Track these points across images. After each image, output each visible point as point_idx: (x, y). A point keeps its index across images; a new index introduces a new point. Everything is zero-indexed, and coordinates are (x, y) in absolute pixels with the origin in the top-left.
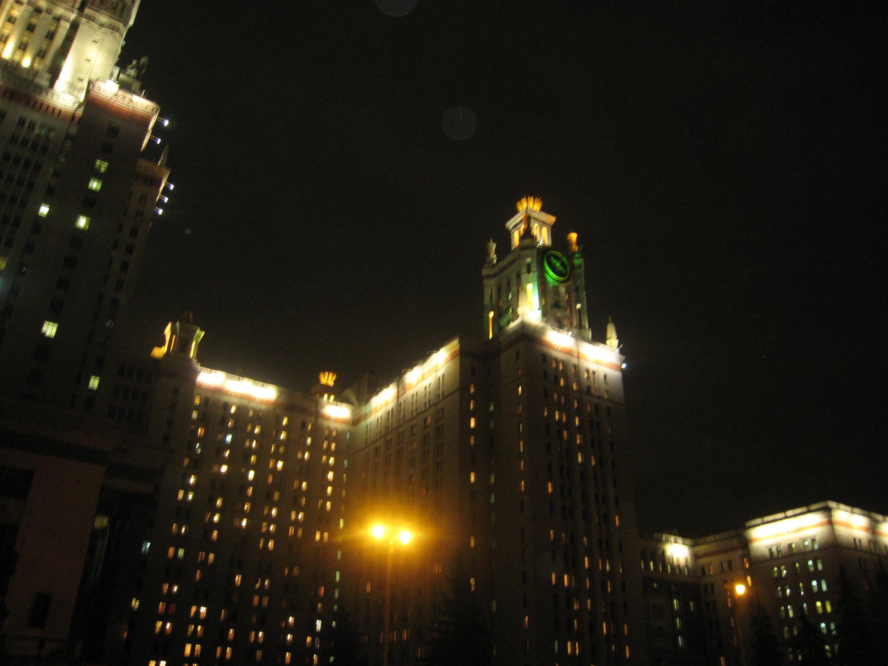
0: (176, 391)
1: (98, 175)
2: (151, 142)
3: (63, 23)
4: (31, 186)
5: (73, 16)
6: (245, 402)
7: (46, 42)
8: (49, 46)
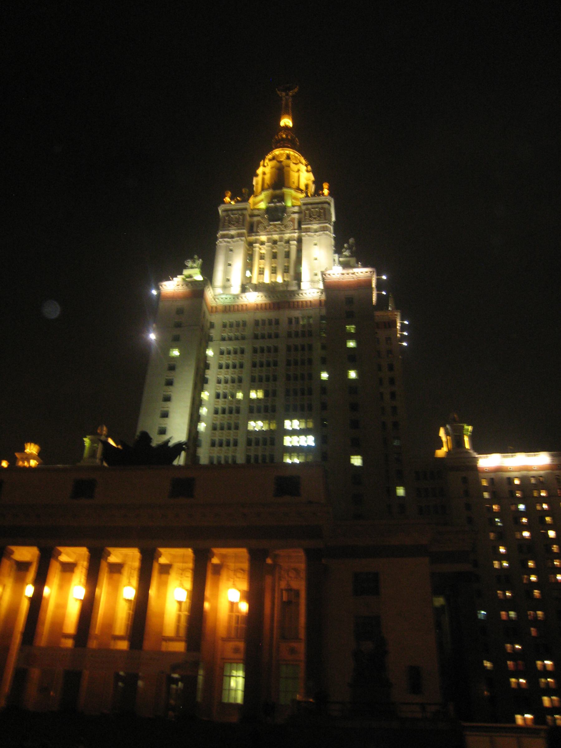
0: (465, 480)
1: (351, 336)
2: (379, 296)
3: (291, 242)
4: (310, 362)
5: (296, 235)
6: (524, 473)
7: (286, 259)
8: (289, 262)
